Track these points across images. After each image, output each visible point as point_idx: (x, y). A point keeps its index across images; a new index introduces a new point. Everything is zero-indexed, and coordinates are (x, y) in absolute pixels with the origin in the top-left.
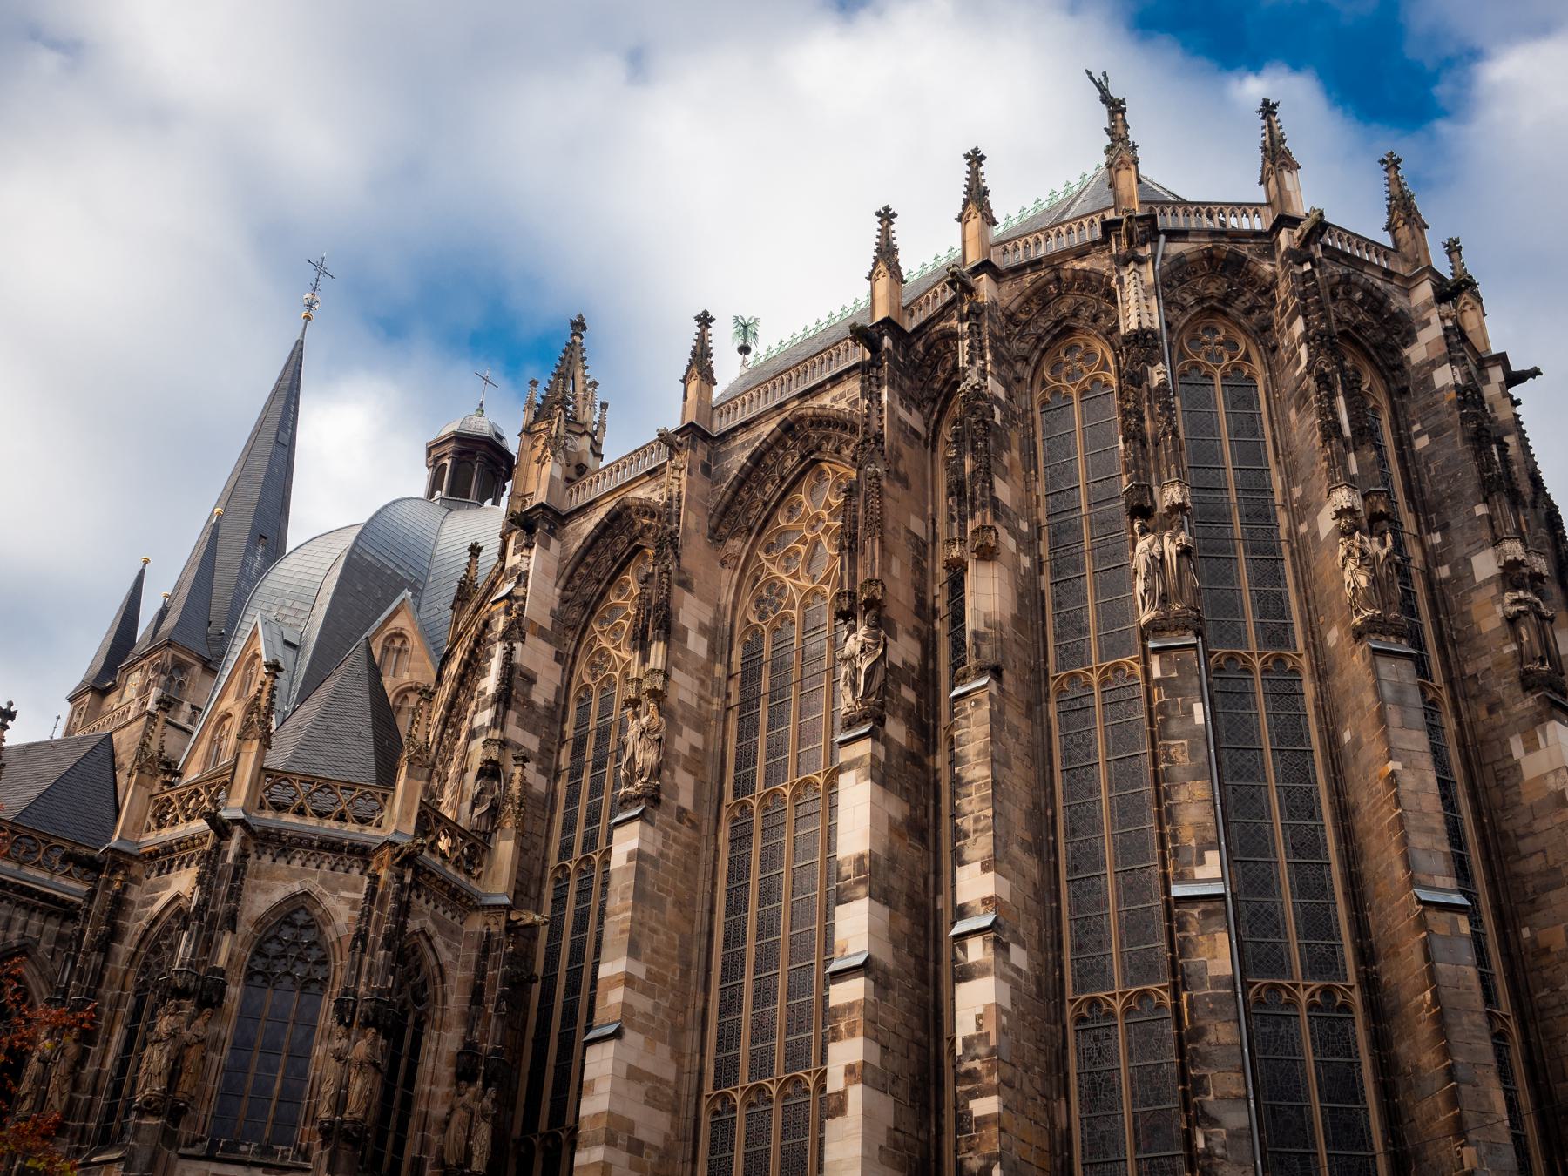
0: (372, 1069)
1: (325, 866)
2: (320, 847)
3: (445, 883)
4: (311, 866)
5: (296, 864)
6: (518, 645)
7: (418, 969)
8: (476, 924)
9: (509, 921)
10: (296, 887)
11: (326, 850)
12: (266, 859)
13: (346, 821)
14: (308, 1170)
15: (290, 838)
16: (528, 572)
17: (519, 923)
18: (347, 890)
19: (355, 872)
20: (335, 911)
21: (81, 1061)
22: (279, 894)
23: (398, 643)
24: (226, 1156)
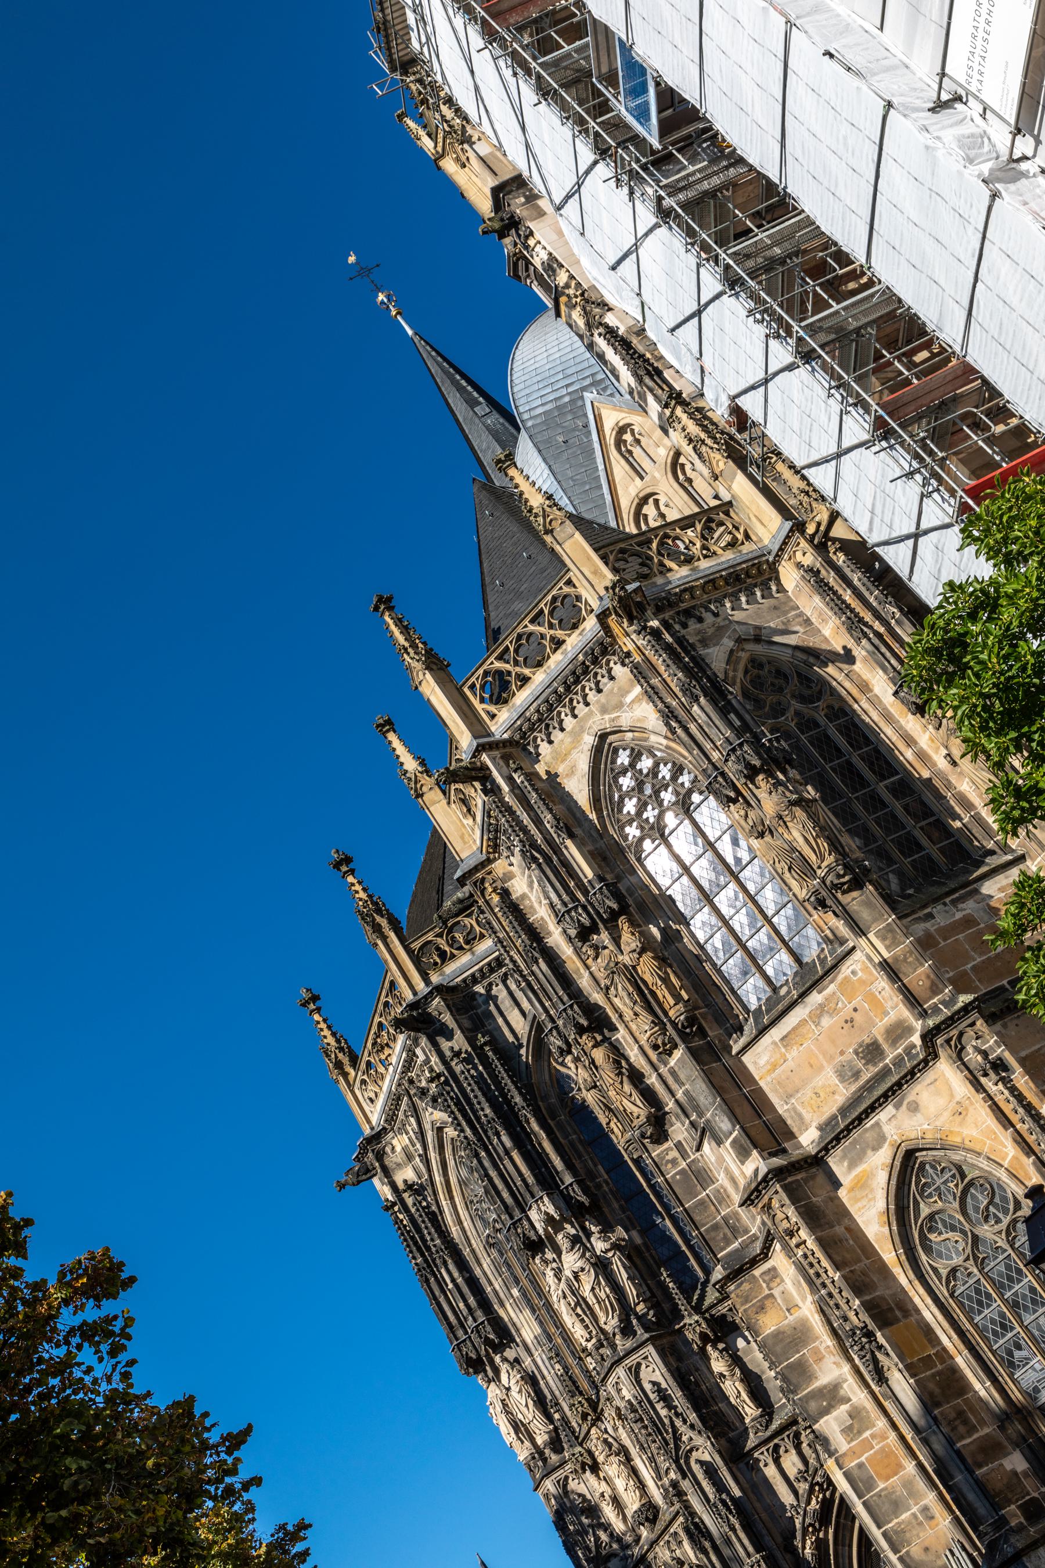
0: (798, 811)
1: (592, 696)
2: (568, 689)
3: (713, 581)
4: (581, 709)
5: (569, 722)
6: (610, 319)
7: (779, 673)
8: (789, 576)
9: (811, 540)
10: (589, 740)
11: (577, 681)
12: (544, 748)
13: (564, 641)
14: (854, 948)
15: (538, 711)
16: (550, 254)
17: (822, 528)
18: (628, 692)
19: (618, 670)
20: (639, 720)
21: (617, 1054)
22: (583, 762)
23: (628, 437)
24: (775, 1013)
